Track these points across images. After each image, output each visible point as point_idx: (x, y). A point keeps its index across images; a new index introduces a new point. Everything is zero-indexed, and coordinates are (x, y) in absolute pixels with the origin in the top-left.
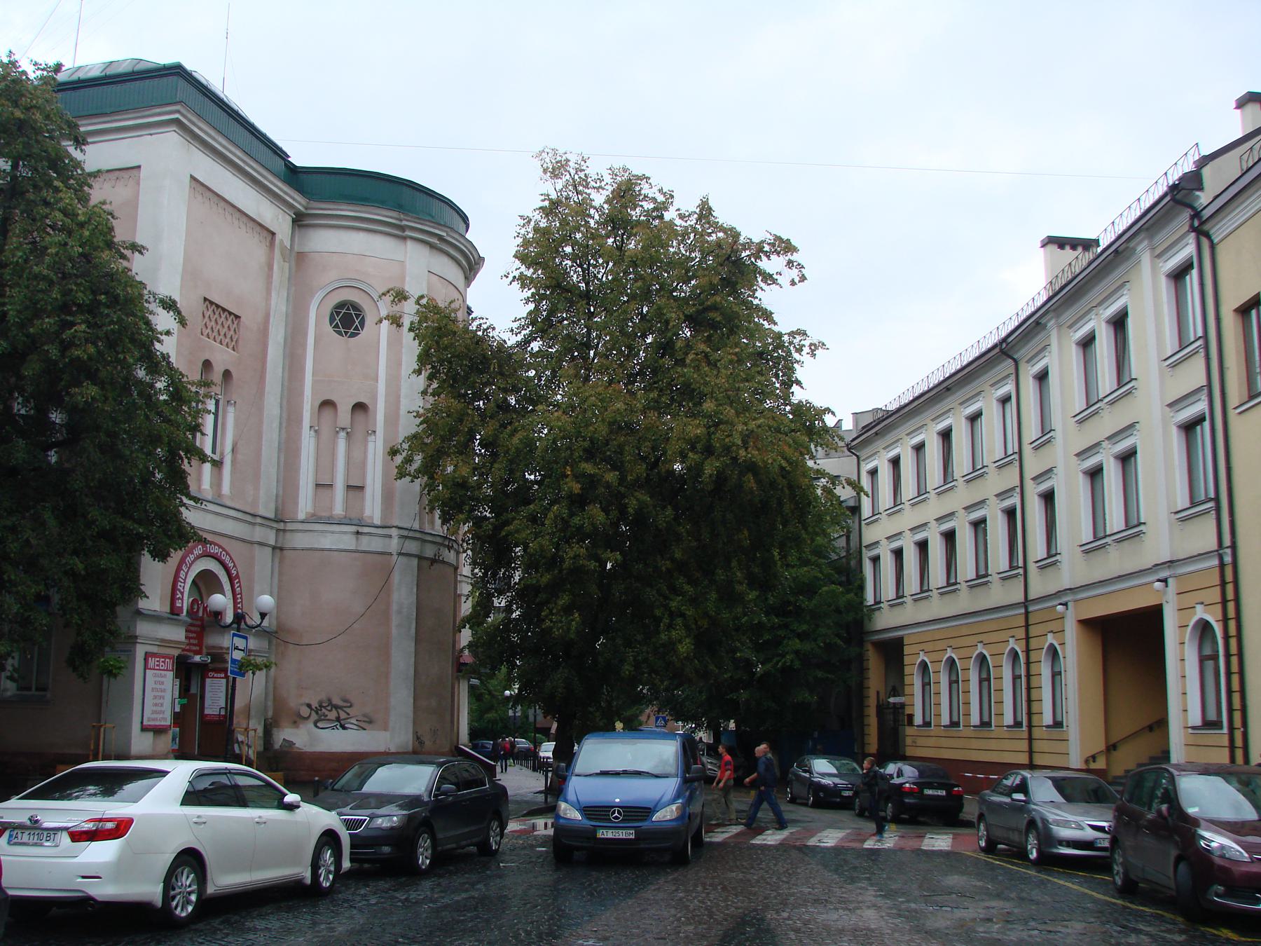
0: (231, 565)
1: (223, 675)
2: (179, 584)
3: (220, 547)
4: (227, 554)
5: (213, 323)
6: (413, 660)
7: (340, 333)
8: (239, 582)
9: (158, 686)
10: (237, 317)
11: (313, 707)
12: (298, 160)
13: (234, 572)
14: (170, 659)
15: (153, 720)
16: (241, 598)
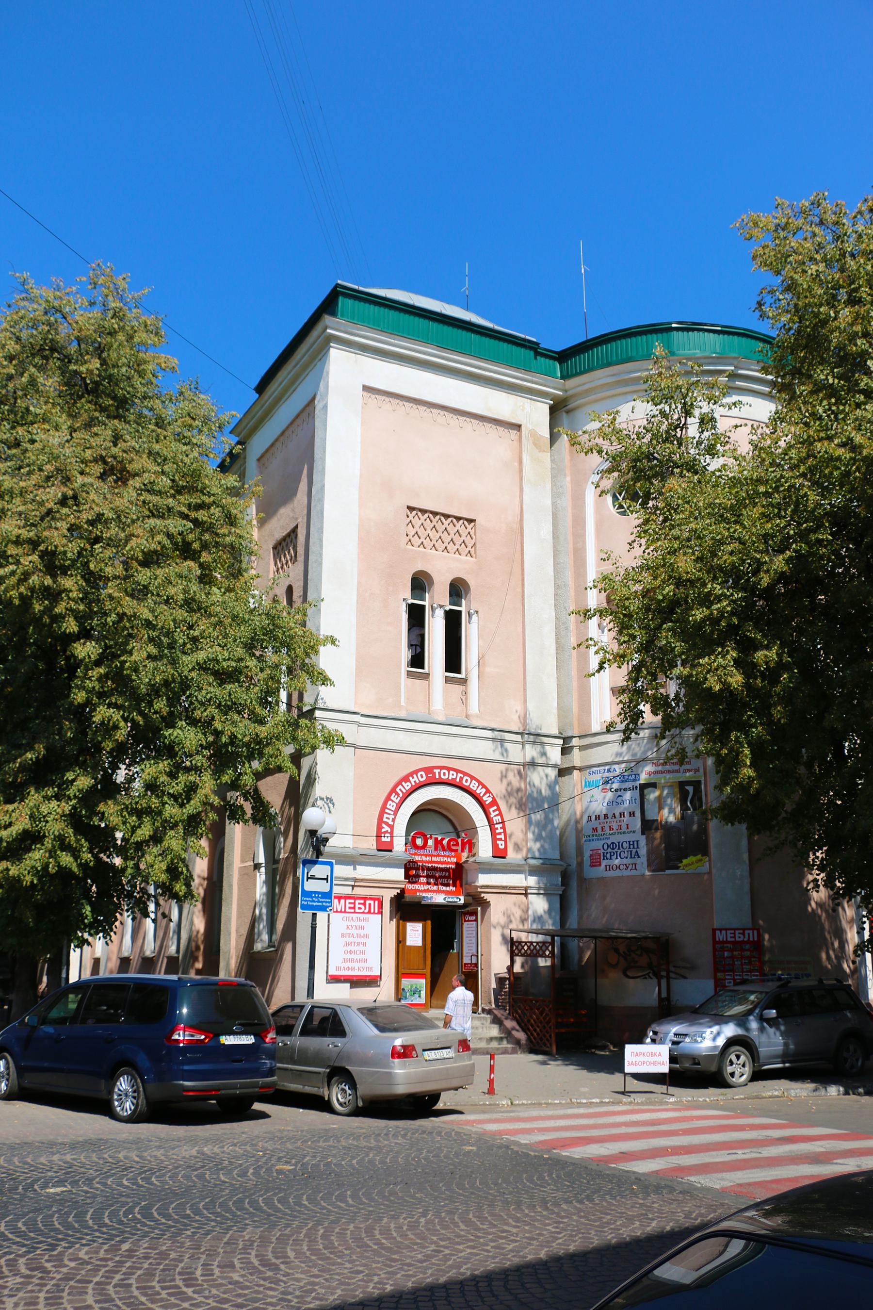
0: (481, 791)
1: (474, 918)
2: (385, 816)
3: (457, 771)
4: (472, 778)
5: (429, 531)
6: (747, 888)
7: (624, 514)
8: (499, 809)
9: (354, 932)
10: (471, 521)
11: (621, 952)
12: (558, 349)
13: (488, 799)
14: (374, 899)
15: (348, 969)
16: (504, 828)
